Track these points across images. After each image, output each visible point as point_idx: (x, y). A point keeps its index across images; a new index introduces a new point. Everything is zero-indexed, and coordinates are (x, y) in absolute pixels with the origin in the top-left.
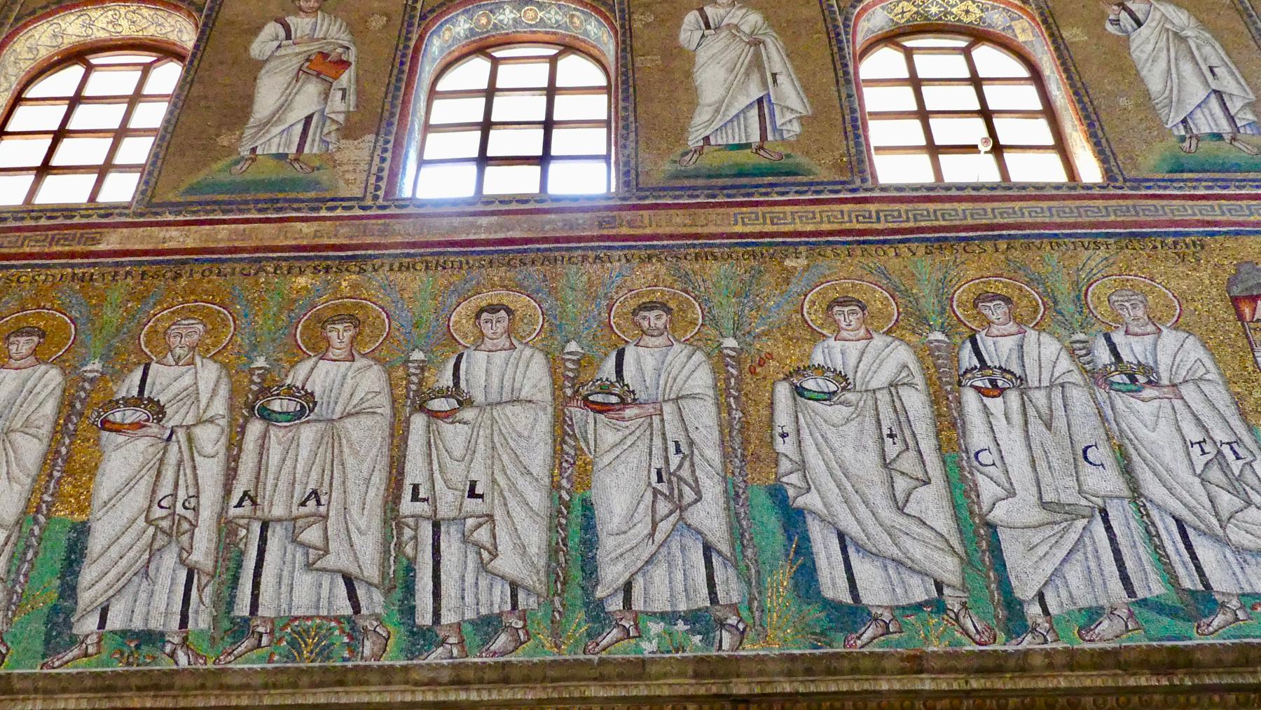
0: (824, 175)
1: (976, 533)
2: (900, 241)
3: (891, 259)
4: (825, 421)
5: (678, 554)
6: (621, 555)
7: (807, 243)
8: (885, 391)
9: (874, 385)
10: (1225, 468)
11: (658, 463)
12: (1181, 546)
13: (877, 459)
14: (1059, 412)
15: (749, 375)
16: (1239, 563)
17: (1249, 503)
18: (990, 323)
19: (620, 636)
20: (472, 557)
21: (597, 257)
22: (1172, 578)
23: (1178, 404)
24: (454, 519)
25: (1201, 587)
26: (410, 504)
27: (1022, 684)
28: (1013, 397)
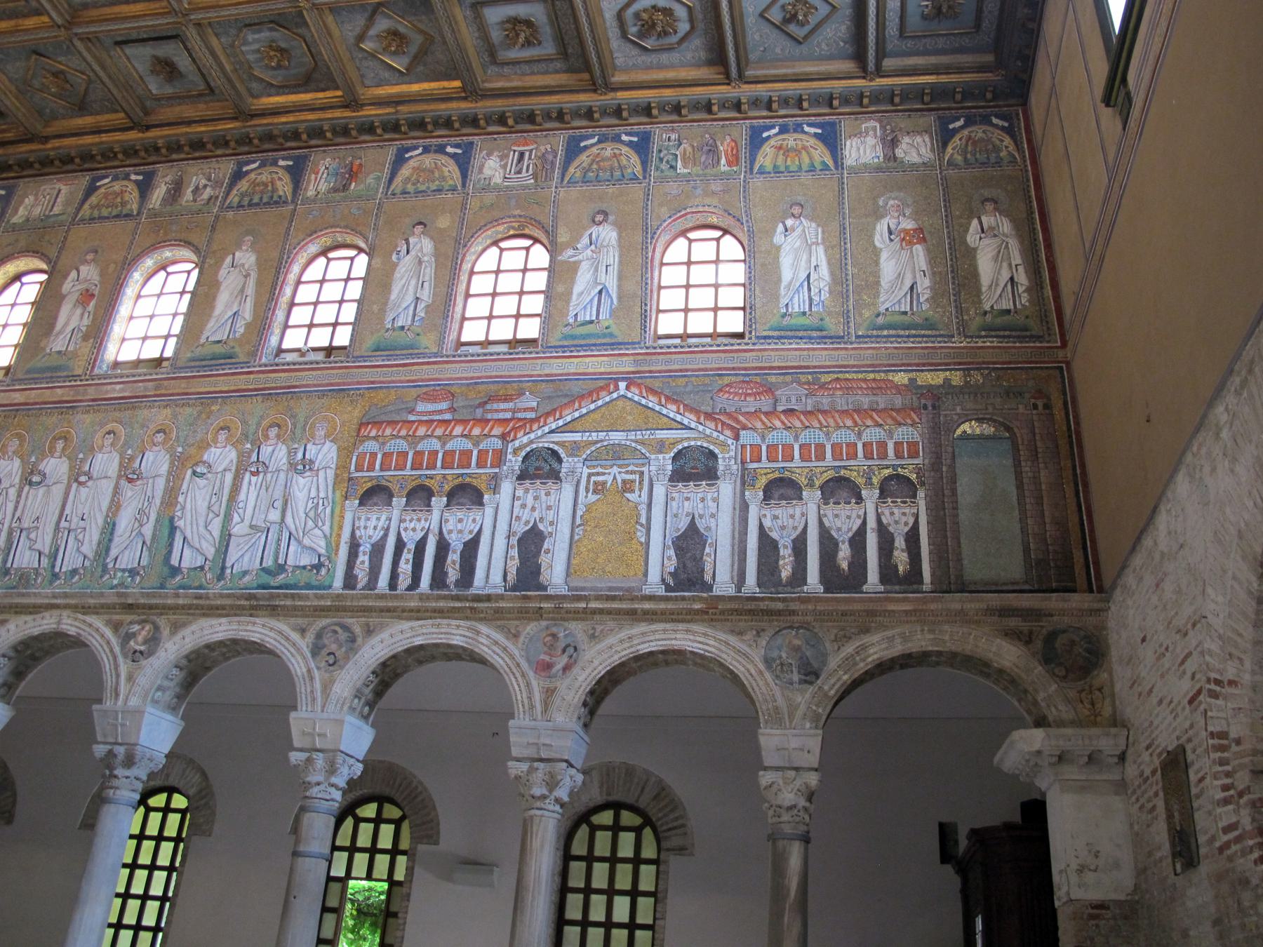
0: (242, 358)
22: (276, 558)
28: (261, 475)
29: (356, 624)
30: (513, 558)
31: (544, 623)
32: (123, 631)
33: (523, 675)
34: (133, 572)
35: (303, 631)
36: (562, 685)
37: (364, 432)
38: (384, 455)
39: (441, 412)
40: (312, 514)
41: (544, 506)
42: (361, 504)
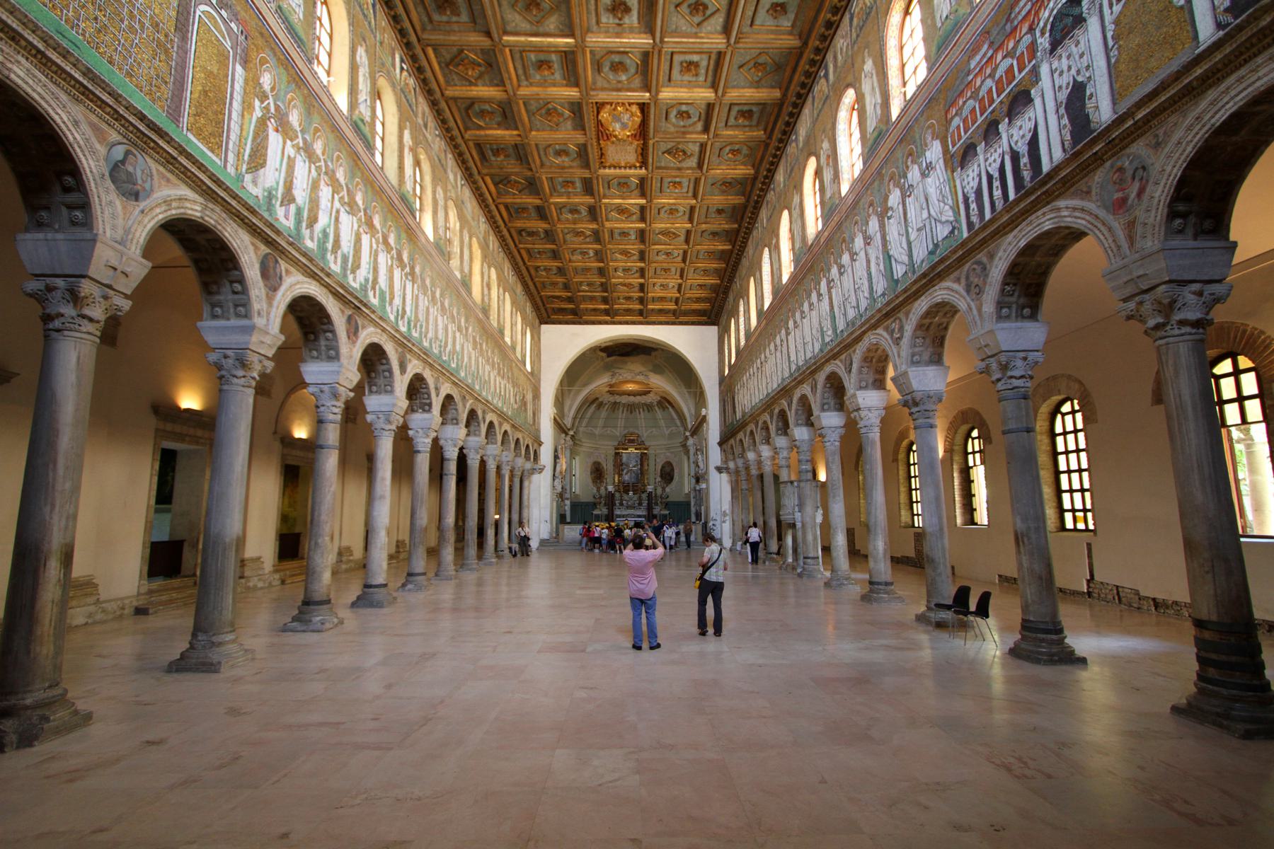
29: (982, 257)
30: (1065, 126)
31: (1108, 164)
33: (1104, 224)
34: (883, 295)
35: (958, 280)
36: (1139, 213)
37: (949, 116)
38: (965, 121)
41: (1077, 57)
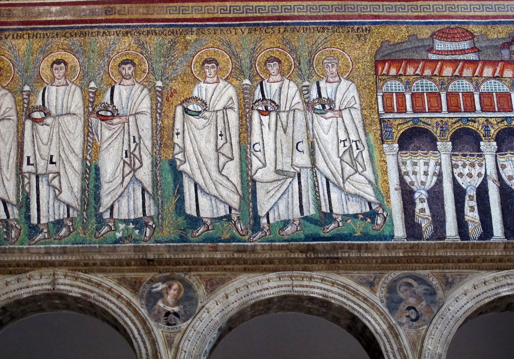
1: (248, 185)
2: (239, 25)
3: (233, 37)
4: (195, 127)
5: (132, 192)
6: (110, 192)
7: (197, 26)
8: (221, 112)
9: (217, 108)
10: (351, 153)
11: (126, 148)
12: (326, 192)
13: (214, 147)
14: (290, 125)
15: (166, 102)
16: (346, 200)
17: (356, 171)
18: (270, 74)
19: (108, 230)
20: (52, 192)
21: (104, 33)
22: (319, 207)
23: (340, 120)
24: (45, 174)
25: (329, 211)
26: (27, 166)
27: (253, 256)
28: (273, 115)
32: (143, 290)
34: (139, 223)
35: (371, 285)
38: (413, 95)
39: (463, 52)
40: (347, 158)
42: (401, 148)
